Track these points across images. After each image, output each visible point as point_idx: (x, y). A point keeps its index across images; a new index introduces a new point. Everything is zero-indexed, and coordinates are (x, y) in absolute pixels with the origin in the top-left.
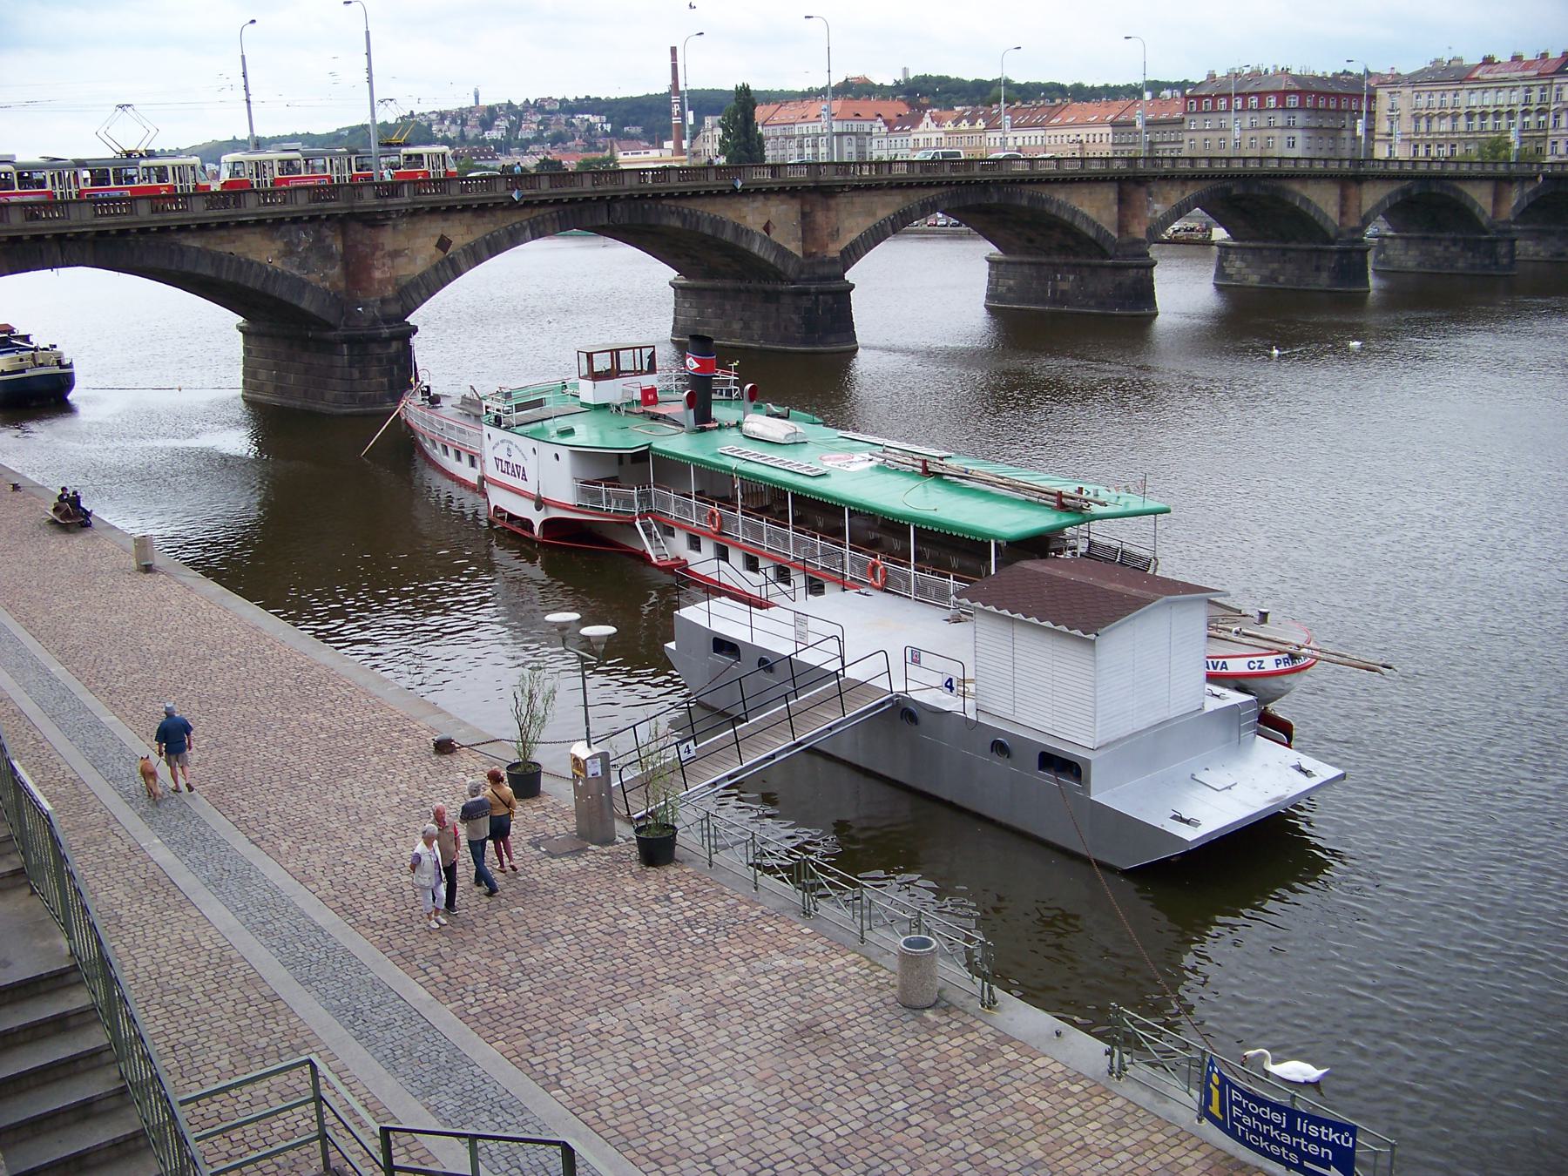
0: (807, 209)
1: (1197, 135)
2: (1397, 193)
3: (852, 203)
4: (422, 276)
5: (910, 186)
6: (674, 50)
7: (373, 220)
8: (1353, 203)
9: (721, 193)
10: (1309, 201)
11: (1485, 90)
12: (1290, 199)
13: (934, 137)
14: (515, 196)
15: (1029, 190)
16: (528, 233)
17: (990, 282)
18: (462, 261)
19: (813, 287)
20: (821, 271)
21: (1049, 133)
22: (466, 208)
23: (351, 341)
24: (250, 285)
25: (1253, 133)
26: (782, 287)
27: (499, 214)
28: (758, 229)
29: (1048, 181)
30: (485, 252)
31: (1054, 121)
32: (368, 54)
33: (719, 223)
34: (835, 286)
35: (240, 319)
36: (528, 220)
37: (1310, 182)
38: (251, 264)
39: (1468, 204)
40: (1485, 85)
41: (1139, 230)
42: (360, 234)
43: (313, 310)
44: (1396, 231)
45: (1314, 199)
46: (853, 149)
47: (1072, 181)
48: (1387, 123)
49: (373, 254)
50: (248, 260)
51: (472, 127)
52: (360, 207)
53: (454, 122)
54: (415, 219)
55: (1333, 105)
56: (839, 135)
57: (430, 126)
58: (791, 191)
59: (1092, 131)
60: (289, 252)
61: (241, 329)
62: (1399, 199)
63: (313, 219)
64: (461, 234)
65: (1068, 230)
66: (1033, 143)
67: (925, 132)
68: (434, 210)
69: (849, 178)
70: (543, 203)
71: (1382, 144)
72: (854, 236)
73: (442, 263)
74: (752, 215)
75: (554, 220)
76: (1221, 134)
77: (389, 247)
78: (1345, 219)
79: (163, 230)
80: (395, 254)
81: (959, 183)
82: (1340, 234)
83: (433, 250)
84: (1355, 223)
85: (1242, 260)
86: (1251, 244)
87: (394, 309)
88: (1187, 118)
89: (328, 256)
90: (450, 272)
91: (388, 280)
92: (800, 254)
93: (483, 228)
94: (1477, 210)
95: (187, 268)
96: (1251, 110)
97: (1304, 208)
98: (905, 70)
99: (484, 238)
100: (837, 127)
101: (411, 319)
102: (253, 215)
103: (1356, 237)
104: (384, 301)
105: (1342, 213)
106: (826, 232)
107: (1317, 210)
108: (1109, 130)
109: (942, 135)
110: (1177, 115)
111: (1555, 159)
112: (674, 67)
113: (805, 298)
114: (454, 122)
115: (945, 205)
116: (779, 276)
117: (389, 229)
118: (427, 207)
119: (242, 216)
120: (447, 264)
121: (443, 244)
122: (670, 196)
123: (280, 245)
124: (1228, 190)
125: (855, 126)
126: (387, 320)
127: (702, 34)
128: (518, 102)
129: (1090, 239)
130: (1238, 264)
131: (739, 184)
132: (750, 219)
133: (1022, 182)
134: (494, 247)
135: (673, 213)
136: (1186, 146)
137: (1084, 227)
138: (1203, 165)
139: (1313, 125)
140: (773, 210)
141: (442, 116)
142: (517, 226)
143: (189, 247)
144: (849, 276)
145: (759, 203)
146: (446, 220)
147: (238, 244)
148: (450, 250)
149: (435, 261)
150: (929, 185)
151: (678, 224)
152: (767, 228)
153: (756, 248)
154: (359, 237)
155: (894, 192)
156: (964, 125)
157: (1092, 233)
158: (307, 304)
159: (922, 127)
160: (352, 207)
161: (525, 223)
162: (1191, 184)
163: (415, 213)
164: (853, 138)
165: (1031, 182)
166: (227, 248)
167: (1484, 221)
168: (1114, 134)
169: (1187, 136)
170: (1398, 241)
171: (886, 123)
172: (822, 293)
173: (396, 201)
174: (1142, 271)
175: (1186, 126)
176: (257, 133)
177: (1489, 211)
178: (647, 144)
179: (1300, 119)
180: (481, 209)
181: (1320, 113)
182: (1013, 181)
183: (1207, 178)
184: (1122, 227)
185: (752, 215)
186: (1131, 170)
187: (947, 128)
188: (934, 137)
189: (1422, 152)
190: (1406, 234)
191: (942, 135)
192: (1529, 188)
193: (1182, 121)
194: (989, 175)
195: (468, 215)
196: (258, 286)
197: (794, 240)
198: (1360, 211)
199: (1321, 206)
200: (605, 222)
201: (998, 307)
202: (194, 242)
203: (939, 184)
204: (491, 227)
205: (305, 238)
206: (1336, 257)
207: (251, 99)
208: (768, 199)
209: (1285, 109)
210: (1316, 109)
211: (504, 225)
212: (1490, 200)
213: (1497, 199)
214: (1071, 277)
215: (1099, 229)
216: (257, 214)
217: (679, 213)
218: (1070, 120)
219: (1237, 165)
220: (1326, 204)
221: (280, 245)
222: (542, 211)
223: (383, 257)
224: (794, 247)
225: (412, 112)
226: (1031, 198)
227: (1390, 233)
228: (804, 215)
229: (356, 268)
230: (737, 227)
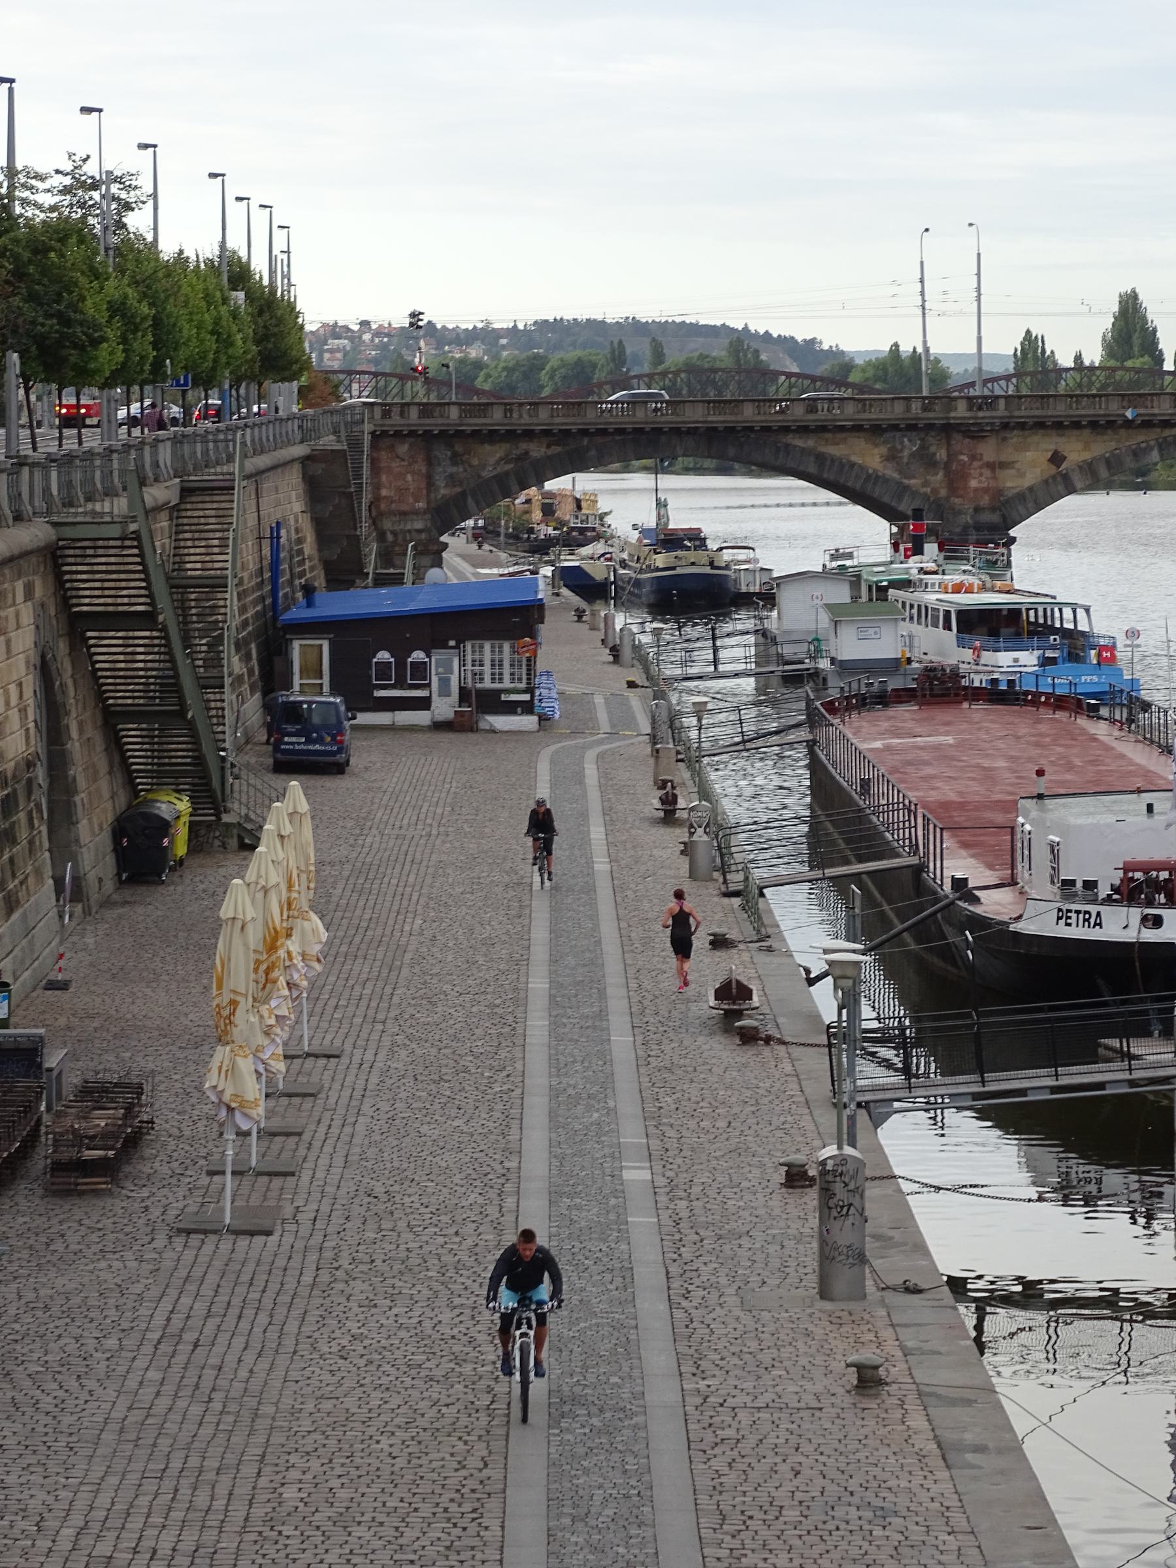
4: (1031, 489)
7: (974, 432)
24: (849, 484)
27: (1123, 432)
32: (978, 274)
36: (1157, 439)
38: (853, 465)
42: (960, 442)
50: (849, 461)
52: (954, 418)
60: (892, 457)
63: (912, 428)
64: (1076, 451)
68: (1058, 426)
73: (1054, 477)
79: (767, 429)
87: (994, 518)
89: (931, 463)
91: (986, 490)
99: (1103, 455)
118: (1030, 421)
120: (1059, 479)
121: (1057, 459)
123: (883, 450)
142: (1143, 445)
143: (795, 446)
146: (1062, 435)
148: (1064, 466)
149: (1045, 476)
160: (948, 418)
173: (994, 414)
202: (798, 442)
204: (1113, 445)
205: (909, 446)
207: (927, 305)
211: (1128, 444)
221: (883, 450)
229: (956, 479)
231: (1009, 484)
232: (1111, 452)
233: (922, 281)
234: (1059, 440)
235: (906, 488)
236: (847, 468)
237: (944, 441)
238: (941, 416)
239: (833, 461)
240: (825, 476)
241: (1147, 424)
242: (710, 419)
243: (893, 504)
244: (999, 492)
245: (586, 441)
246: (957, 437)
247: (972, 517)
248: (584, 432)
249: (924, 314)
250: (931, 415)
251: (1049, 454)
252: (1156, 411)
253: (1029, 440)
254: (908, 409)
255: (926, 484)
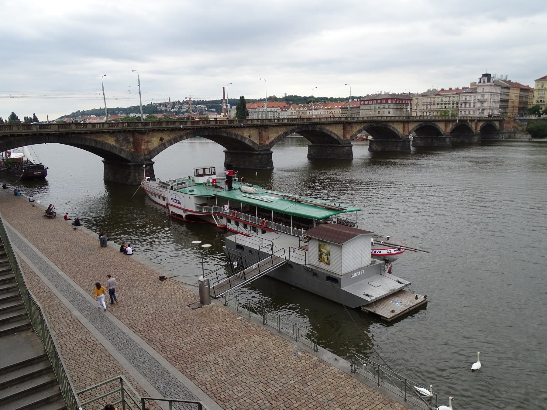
0: (260, 132)
1: (363, 111)
2: (418, 125)
3: (272, 130)
4: (156, 148)
5: (287, 125)
6: (224, 88)
7: (142, 132)
8: (406, 128)
9: (237, 127)
10: (394, 128)
11: (442, 97)
12: (389, 127)
13: (293, 112)
14: (181, 127)
15: (319, 126)
16: (185, 137)
17: (308, 151)
18: (167, 145)
19: (262, 153)
20: (264, 148)
21: (324, 111)
22: (168, 130)
23: (135, 166)
24: (105, 149)
25: (379, 110)
26: (253, 152)
28: (247, 137)
29: (324, 124)
30: (173, 142)
31: (326, 107)
32: (139, 86)
33: (237, 135)
34: (268, 152)
35: (103, 159)
37: (395, 123)
38: (106, 143)
39: (438, 128)
40: (442, 96)
41: (348, 137)
43: (124, 157)
44: (418, 136)
45: (396, 127)
46: (272, 116)
47: (331, 124)
48: (416, 107)
49: (142, 142)
50: (105, 142)
51: (169, 108)
52: (137, 129)
53: (164, 106)
54: (154, 132)
55: (401, 102)
56: (268, 111)
57: (157, 107)
58: (256, 127)
59: (335, 110)
60: (117, 141)
61: (103, 161)
62: (419, 127)
63: (124, 132)
64: (166, 137)
65: (330, 137)
66: (320, 113)
67: (291, 111)
68: (159, 130)
69: (272, 123)
70: (189, 129)
71: (414, 112)
72: (273, 139)
73: (161, 144)
74: (246, 133)
75: (192, 134)
76: (370, 111)
77: (146, 140)
78: (404, 133)
80: (148, 142)
81: (300, 125)
82: (403, 137)
83: (158, 141)
84: (407, 134)
85: (376, 144)
86: (379, 140)
87: (148, 157)
88: (361, 106)
89: (128, 142)
90: (163, 147)
91: (146, 149)
92: (258, 144)
93: (172, 136)
94: (440, 130)
95: (87, 144)
96: (378, 104)
97: (393, 130)
98: (286, 94)
100: (268, 109)
101: (153, 160)
102: (106, 130)
103: (407, 137)
104: (145, 155)
105: (403, 131)
106: (265, 138)
107: (397, 130)
108: (340, 110)
109: (295, 112)
110: (358, 106)
111: (461, 116)
112: (224, 93)
113: (260, 155)
114: (164, 106)
115: (297, 130)
116: (253, 149)
117: (146, 135)
118: (157, 129)
119: (103, 130)
120: (162, 145)
121: (161, 139)
122: (224, 128)
124: (373, 125)
125: (272, 109)
126: (146, 160)
127: (232, 83)
128: (181, 101)
129: (335, 139)
130: (375, 145)
131: (242, 125)
132: (245, 134)
133: (317, 124)
134: (176, 141)
135: (224, 132)
136: (361, 114)
137: (334, 136)
138: (366, 119)
139: (395, 107)
140: (251, 132)
141: (160, 104)
142: (182, 135)
144: (272, 150)
145: (247, 130)
146: (162, 133)
147: (102, 138)
148: (163, 141)
150: (293, 125)
151: (226, 135)
152: (249, 137)
153: (247, 142)
154: (137, 137)
155: (284, 127)
156: (301, 109)
157: (336, 138)
158: (123, 155)
159: (290, 109)
160: (135, 129)
161: (184, 134)
162: (362, 124)
163: (153, 131)
164: (272, 112)
165: (320, 124)
166: (100, 139)
167: (442, 133)
168: (341, 111)
169: (361, 111)
170: (418, 138)
171: (281, 108)
172: (264, 154)
173: (148, 127)
174: (349, 148)
175: (361, 108)
176: (107, 107)
177: (444, 130)
178: (217, 113)
179: (392, 106)
180: (172, 130)
181: (397, 104)
182: (315, 124)
183: (367, 122)
184: (344, 136)
185: (246, 133)
186: (347, 120)
187: (297, 110)
188: (293, 112)
189: (425, 114)
190: (421, 137)
191: (295, 112)
192: (454, 124)
193: (359, 107)
194: (309, 122)
195: (168, 132)
196: (108, 150)
197: (257, 140)
198: (408, 130)
199: (398, 129)
200: (206, 134)
201: (310, 157)
203: (295, 125)
206: (402, 143)
208: (250, 129)
209: (388, 103)
210: (396, 103)
212: (444, 127)
213: (446, 127)
214: (330, 149)
215: (338, 136)
216: (107, 130)
217: (226, 133)
218: (330, 107)
219: (375, 118)
220: (399, 129)
221: (114, 138)
222: (189, 131)
223: (144, 143)
224: (257, 142)
225: (151, 103)
226: (320, 128)
227: (416, 136)
228: (259, 133)
229: (137, 145)
230: (242, 136)
231: (150, 147)
232: (175, 137)
234: (162, 134)
235: (122, 149)
236: (104, 144)
237: (131, 135)
238: (133, 128)
239: (100, 142)
240: (98, 147)
241: (185, 129)
242: (60, 130)
243: (119, 154)
244: (147, 149)
245: (12, 139)
246: (136, 134)
247: (143, 157)
248: (12, 136)
249: (105, 99)
250: (130, 128)
252: (187, 126)
253: (154, 134)
254: (123, 126)
255: (127, 148)
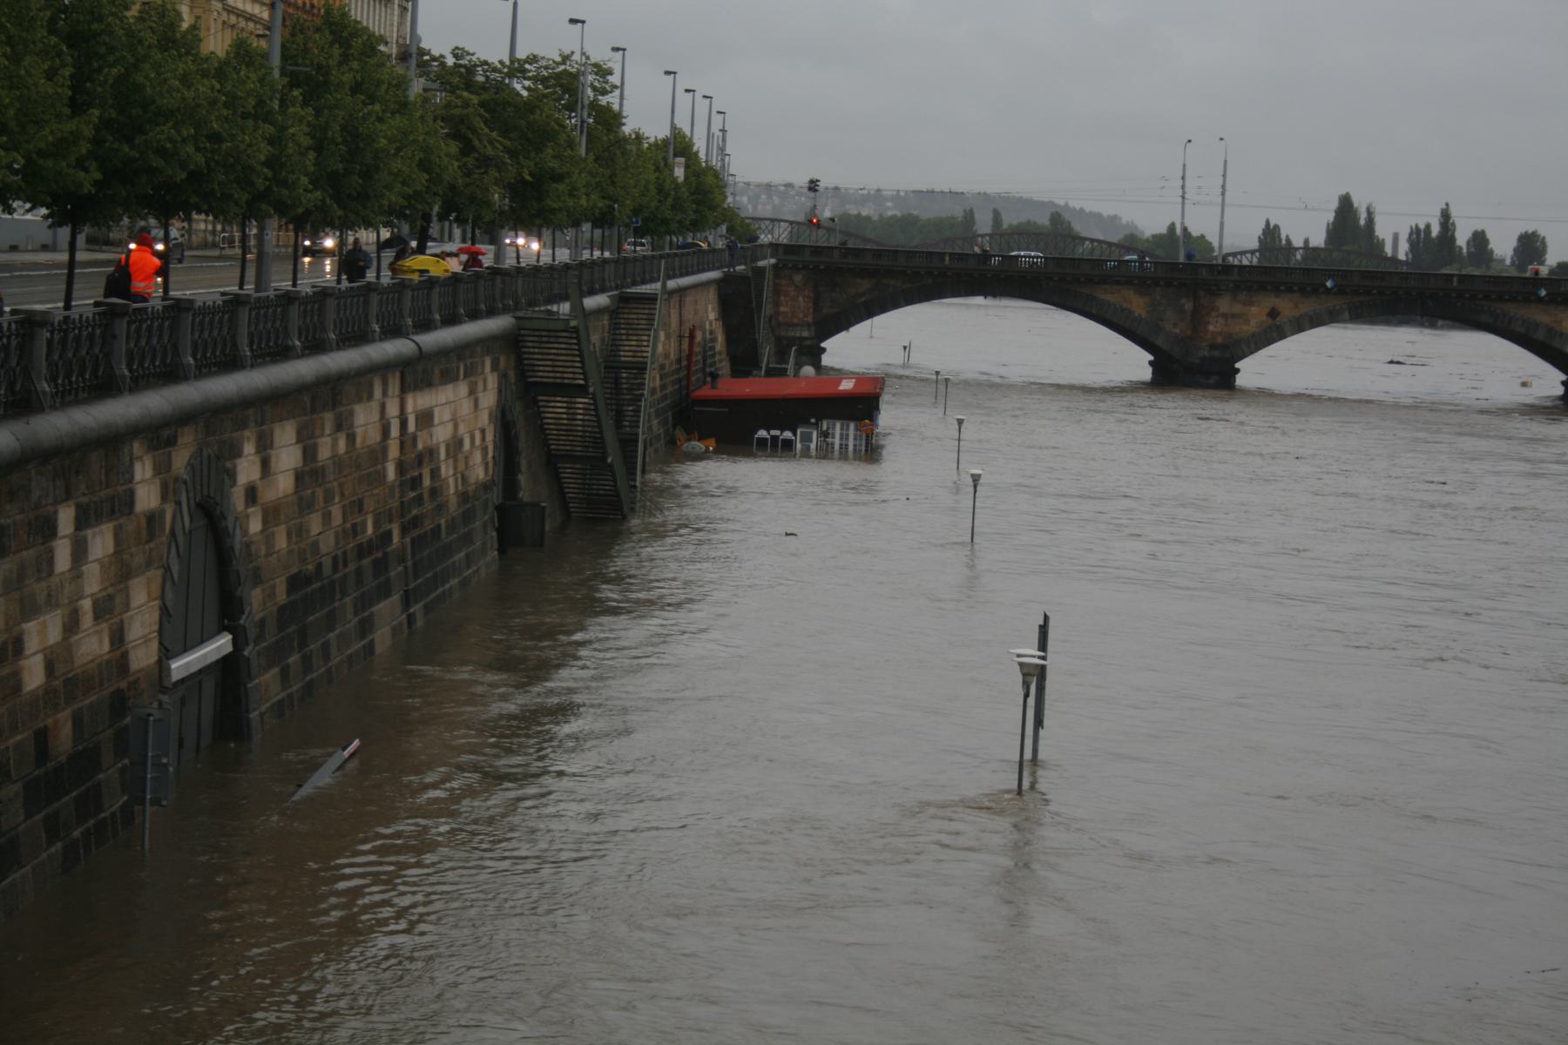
4: (1253, 335)
16: (1346, 315)
32: (1224, 176)
35: (1152, 358)
61: (1151, 363)
64: (1287, 306)
83: (1265, 318)
121: (1273, 313)
142: (1338, 307)
148: (1278, 319)
207: (1186, 196)
223: (1217, 316)
229: (1197, 320)
233: (1183, 178)
249: (1183, 204)
251: (1268, 310)
